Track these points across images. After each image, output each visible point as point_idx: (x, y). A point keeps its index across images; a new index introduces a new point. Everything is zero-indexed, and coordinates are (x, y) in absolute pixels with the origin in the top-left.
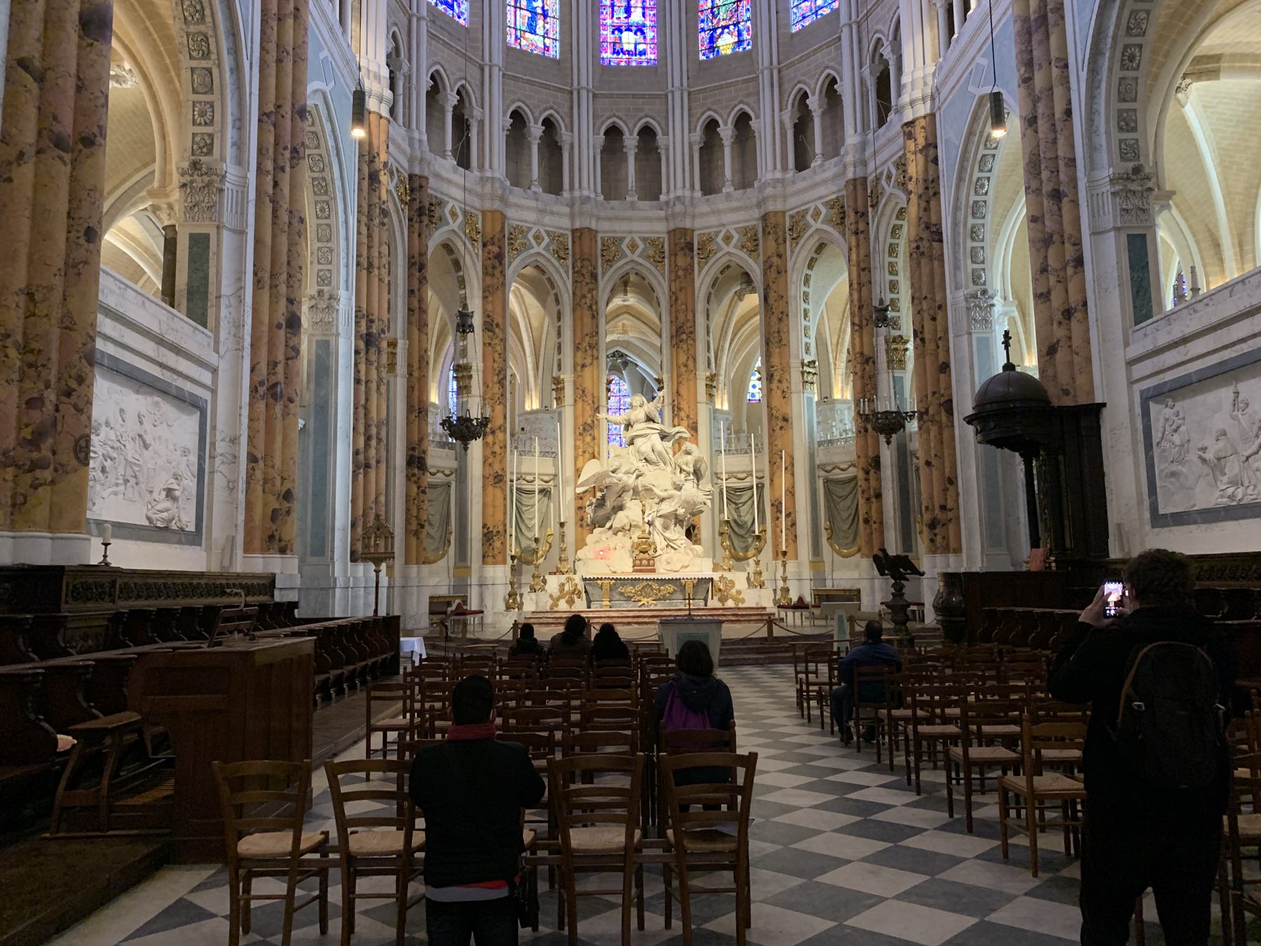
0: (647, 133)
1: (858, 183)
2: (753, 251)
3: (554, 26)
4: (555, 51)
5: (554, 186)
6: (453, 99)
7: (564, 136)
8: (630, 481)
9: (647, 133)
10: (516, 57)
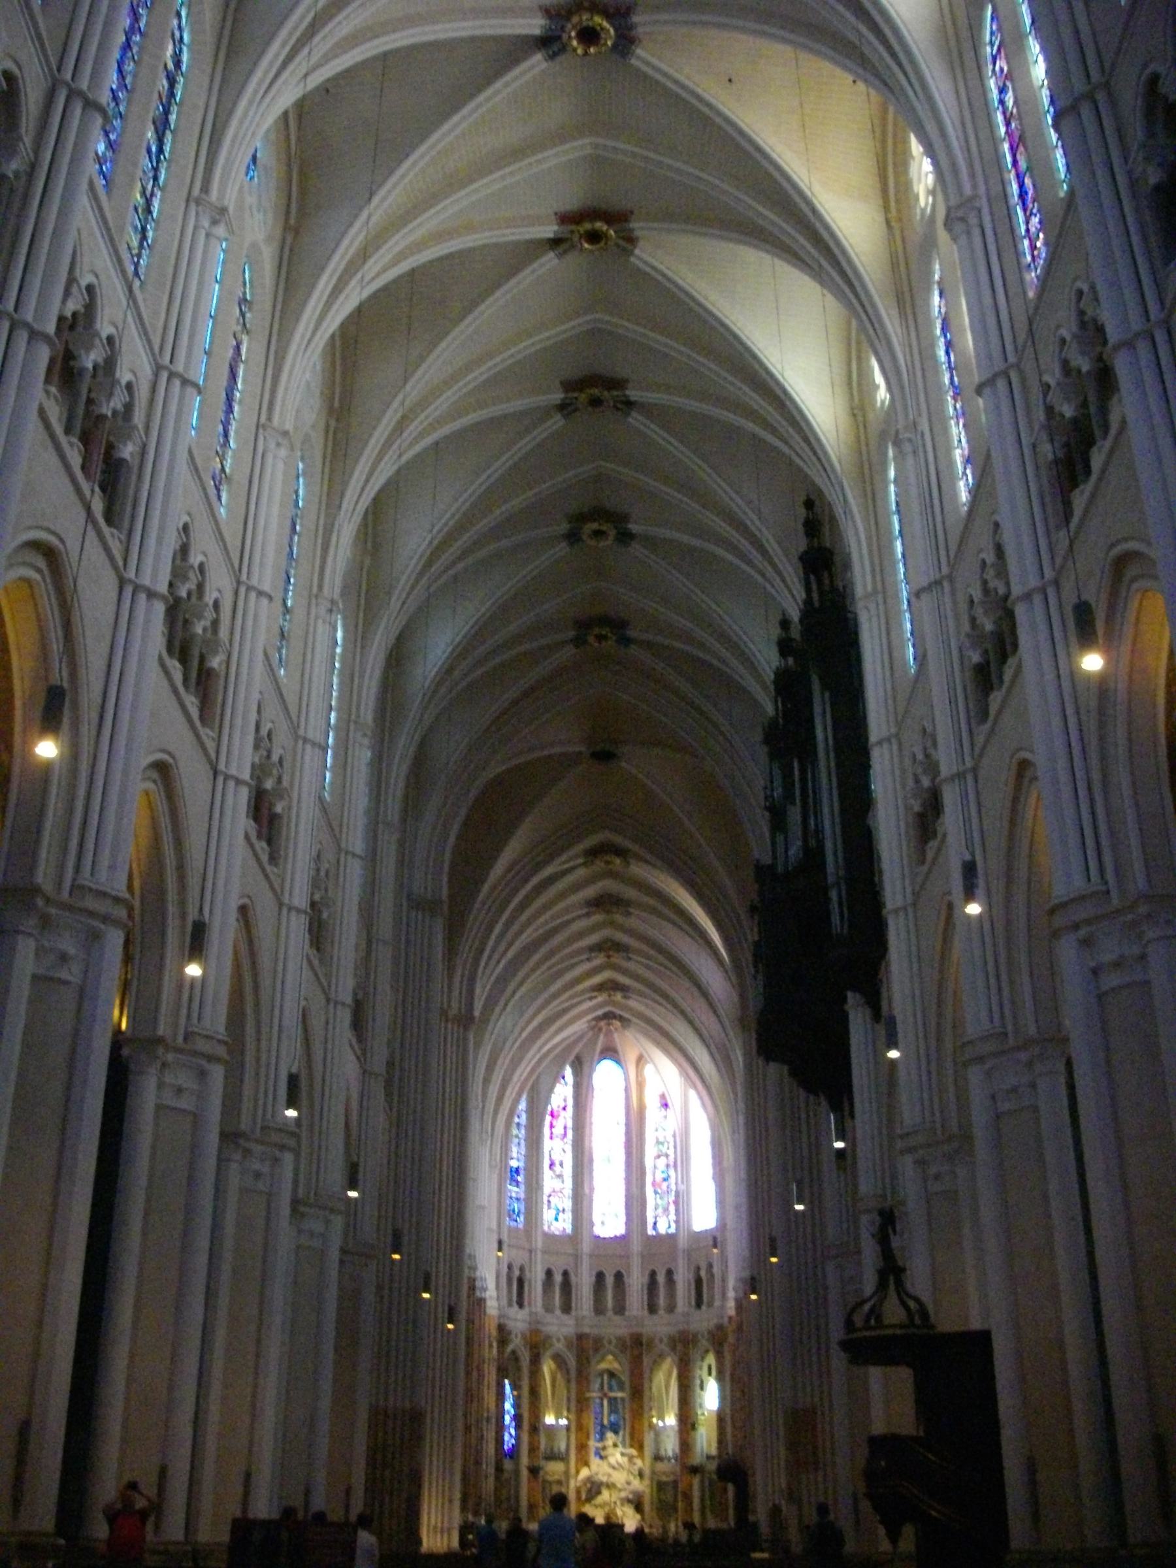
0: (619, 1276)
1: (720, 1327)
2: (674, 1349)
3: (568, 1216)
4: (569, 1230)
5: (567, 1308)
6: (517, 1273)
7: (573, 1279)
8: (604, 1479)
9: (619, 1276)
10: (549, 1237)
